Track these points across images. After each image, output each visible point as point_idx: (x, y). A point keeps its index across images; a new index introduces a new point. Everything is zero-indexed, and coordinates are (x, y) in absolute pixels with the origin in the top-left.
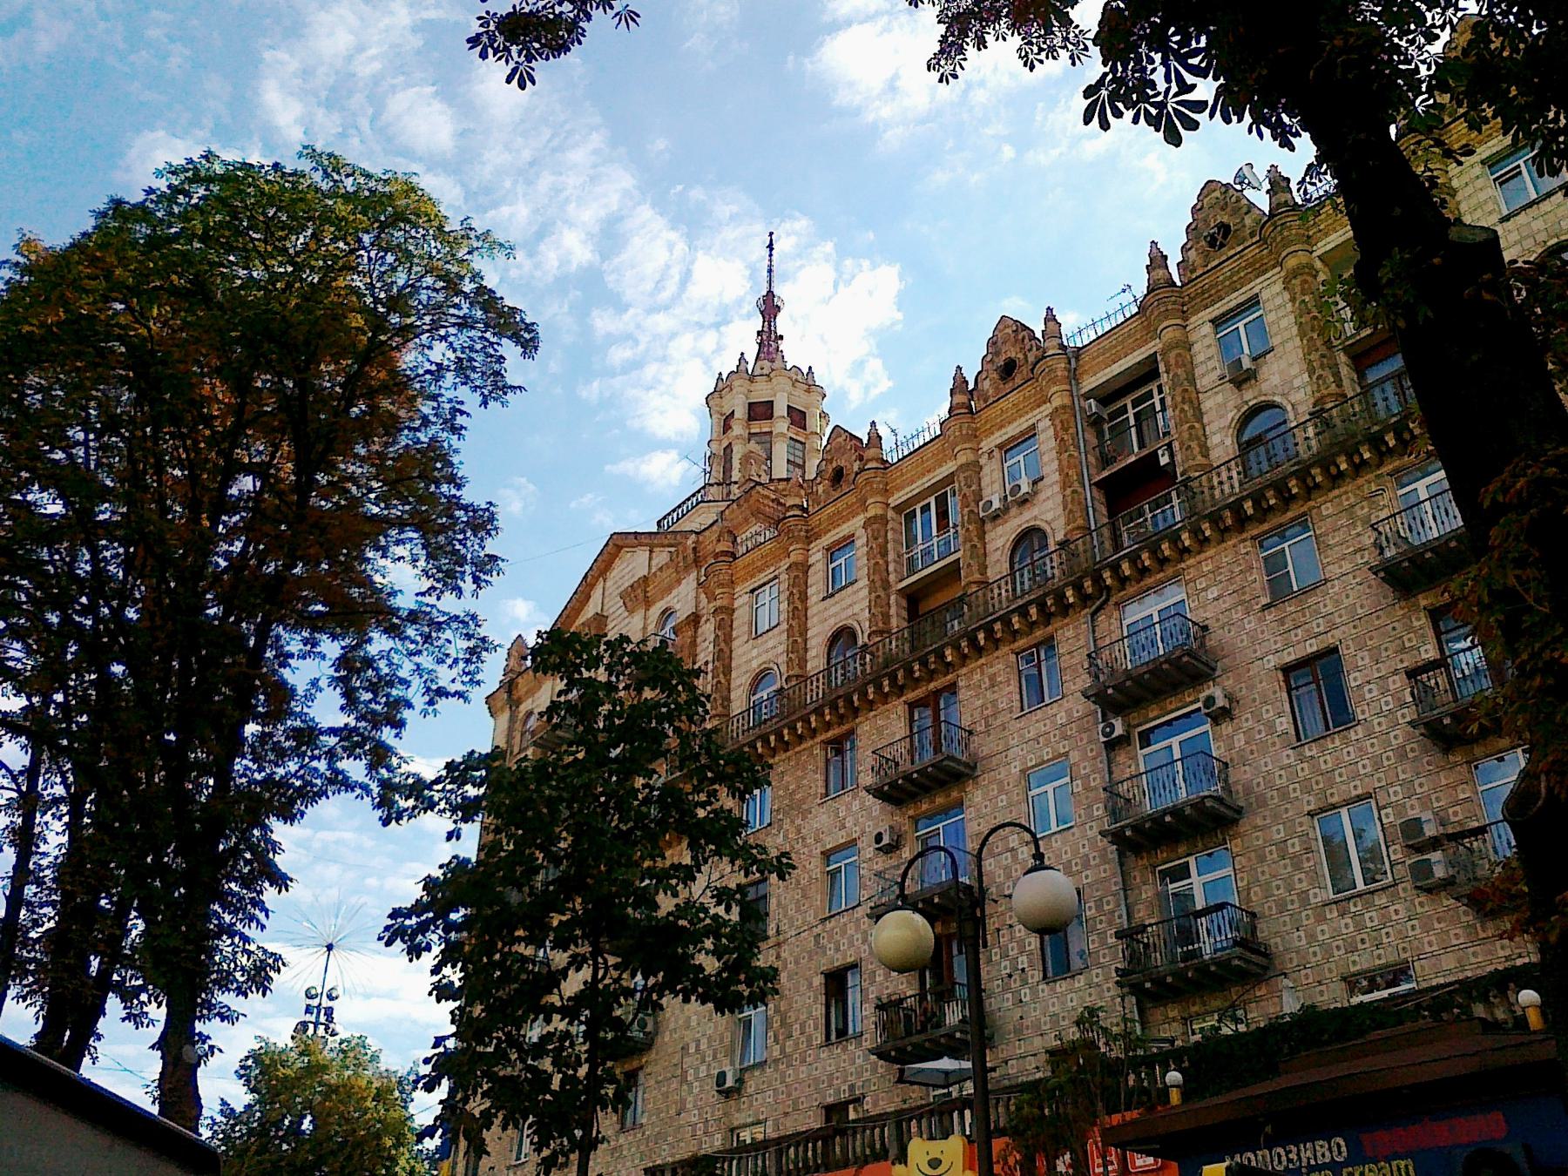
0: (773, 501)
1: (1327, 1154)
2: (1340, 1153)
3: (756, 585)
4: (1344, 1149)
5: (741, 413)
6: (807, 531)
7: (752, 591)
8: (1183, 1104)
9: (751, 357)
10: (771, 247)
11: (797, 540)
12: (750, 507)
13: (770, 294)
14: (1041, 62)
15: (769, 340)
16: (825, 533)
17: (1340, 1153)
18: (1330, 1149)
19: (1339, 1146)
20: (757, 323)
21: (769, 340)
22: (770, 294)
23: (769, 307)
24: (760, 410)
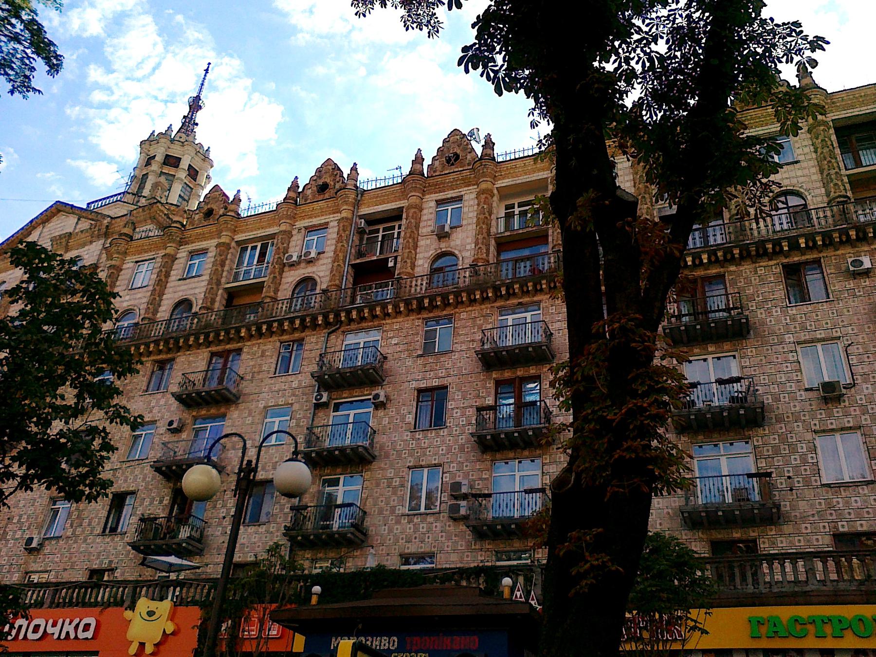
0: (165, 215)
1: (387, 645)
2: (393, 645)
3: (140, 259)
4: (396, 643)
5: (159, 158)
6: (181, 238)
7: (137, 262)
8: (317, 605)
9: (176, 129)
10: (207, 71)
11: (174, 241)
12: (149, 213)
13: (198, 98)
14: (413, 28)
15: (189, 123)
17: (393, 645)
18: (389, 643)
19: (394, 641)
20: (186, 111)
21: (189, 123)
22: (198, 98)
23: (195, 105)
24: (172, 161)
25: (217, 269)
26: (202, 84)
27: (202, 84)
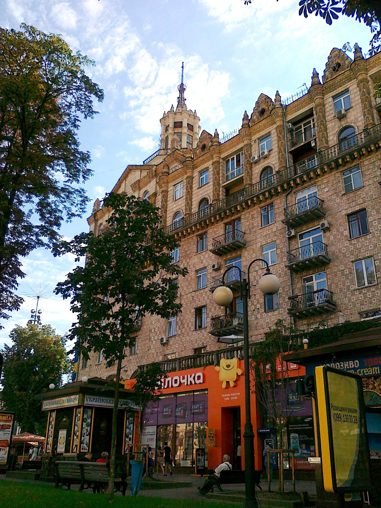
1: (353, 365)
2: (357, 365)
4: (358, 364)
5: (171, 125)
6: (193, 166)
7: (174, 185)
9: (175, 106)
10: (183, 67)
13: (182, 84)
15: (181, 100)
16: (199, 167)
17: (357, 365)
18: (354, 364)
19: (357, 363)
20: (178, 94)
21: (181, 100)
22: (182, 84)
23: (182, 89)
24: (178, 125)
25: (216, 177)
26: (182, 76)
27: (182, 76)
